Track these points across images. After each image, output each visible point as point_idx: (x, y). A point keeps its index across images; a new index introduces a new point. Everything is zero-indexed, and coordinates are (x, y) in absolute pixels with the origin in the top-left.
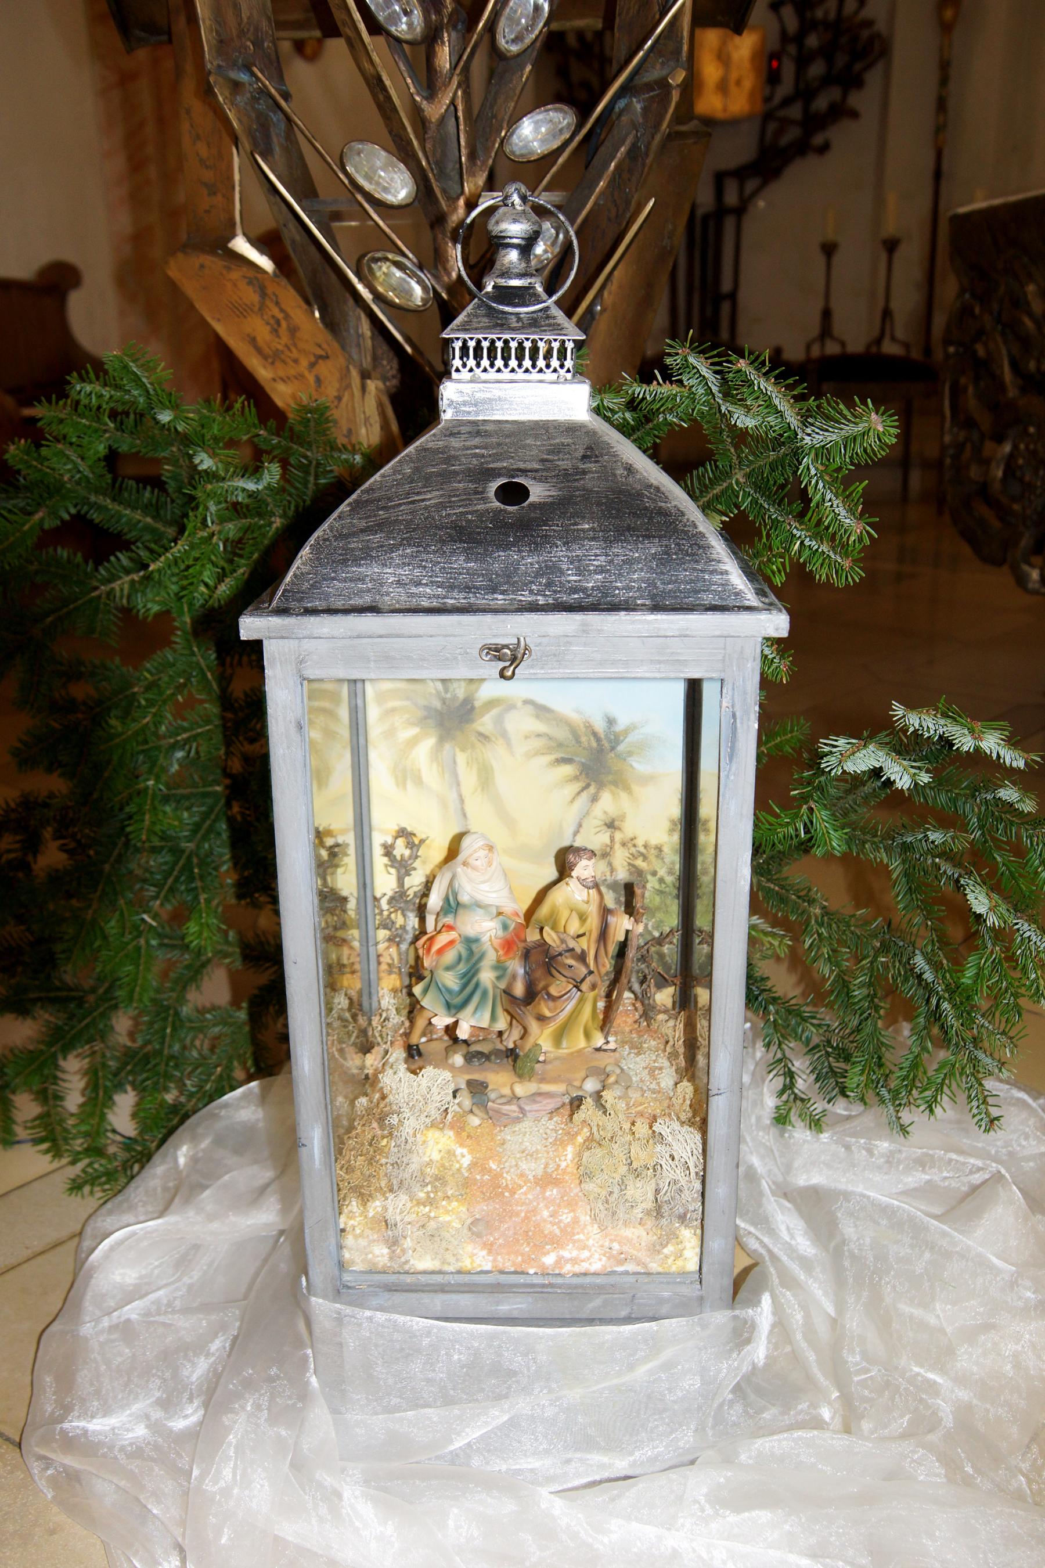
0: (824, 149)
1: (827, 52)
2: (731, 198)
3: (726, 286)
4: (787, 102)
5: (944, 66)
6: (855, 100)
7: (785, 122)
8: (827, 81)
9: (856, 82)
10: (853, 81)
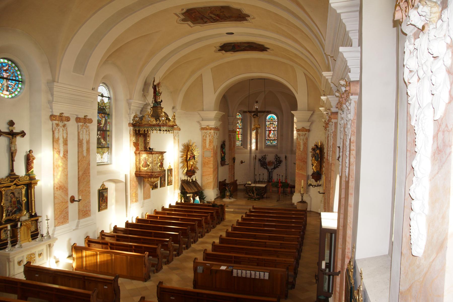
0: (278, 167)
1: (278, 161)
2: (272, 171)
3: (272, 176)
5: (286, 163)
6: (280, 164)
7: (275, 166)
8: (279, 163)
9: (281, 164)
10: (280, 163)
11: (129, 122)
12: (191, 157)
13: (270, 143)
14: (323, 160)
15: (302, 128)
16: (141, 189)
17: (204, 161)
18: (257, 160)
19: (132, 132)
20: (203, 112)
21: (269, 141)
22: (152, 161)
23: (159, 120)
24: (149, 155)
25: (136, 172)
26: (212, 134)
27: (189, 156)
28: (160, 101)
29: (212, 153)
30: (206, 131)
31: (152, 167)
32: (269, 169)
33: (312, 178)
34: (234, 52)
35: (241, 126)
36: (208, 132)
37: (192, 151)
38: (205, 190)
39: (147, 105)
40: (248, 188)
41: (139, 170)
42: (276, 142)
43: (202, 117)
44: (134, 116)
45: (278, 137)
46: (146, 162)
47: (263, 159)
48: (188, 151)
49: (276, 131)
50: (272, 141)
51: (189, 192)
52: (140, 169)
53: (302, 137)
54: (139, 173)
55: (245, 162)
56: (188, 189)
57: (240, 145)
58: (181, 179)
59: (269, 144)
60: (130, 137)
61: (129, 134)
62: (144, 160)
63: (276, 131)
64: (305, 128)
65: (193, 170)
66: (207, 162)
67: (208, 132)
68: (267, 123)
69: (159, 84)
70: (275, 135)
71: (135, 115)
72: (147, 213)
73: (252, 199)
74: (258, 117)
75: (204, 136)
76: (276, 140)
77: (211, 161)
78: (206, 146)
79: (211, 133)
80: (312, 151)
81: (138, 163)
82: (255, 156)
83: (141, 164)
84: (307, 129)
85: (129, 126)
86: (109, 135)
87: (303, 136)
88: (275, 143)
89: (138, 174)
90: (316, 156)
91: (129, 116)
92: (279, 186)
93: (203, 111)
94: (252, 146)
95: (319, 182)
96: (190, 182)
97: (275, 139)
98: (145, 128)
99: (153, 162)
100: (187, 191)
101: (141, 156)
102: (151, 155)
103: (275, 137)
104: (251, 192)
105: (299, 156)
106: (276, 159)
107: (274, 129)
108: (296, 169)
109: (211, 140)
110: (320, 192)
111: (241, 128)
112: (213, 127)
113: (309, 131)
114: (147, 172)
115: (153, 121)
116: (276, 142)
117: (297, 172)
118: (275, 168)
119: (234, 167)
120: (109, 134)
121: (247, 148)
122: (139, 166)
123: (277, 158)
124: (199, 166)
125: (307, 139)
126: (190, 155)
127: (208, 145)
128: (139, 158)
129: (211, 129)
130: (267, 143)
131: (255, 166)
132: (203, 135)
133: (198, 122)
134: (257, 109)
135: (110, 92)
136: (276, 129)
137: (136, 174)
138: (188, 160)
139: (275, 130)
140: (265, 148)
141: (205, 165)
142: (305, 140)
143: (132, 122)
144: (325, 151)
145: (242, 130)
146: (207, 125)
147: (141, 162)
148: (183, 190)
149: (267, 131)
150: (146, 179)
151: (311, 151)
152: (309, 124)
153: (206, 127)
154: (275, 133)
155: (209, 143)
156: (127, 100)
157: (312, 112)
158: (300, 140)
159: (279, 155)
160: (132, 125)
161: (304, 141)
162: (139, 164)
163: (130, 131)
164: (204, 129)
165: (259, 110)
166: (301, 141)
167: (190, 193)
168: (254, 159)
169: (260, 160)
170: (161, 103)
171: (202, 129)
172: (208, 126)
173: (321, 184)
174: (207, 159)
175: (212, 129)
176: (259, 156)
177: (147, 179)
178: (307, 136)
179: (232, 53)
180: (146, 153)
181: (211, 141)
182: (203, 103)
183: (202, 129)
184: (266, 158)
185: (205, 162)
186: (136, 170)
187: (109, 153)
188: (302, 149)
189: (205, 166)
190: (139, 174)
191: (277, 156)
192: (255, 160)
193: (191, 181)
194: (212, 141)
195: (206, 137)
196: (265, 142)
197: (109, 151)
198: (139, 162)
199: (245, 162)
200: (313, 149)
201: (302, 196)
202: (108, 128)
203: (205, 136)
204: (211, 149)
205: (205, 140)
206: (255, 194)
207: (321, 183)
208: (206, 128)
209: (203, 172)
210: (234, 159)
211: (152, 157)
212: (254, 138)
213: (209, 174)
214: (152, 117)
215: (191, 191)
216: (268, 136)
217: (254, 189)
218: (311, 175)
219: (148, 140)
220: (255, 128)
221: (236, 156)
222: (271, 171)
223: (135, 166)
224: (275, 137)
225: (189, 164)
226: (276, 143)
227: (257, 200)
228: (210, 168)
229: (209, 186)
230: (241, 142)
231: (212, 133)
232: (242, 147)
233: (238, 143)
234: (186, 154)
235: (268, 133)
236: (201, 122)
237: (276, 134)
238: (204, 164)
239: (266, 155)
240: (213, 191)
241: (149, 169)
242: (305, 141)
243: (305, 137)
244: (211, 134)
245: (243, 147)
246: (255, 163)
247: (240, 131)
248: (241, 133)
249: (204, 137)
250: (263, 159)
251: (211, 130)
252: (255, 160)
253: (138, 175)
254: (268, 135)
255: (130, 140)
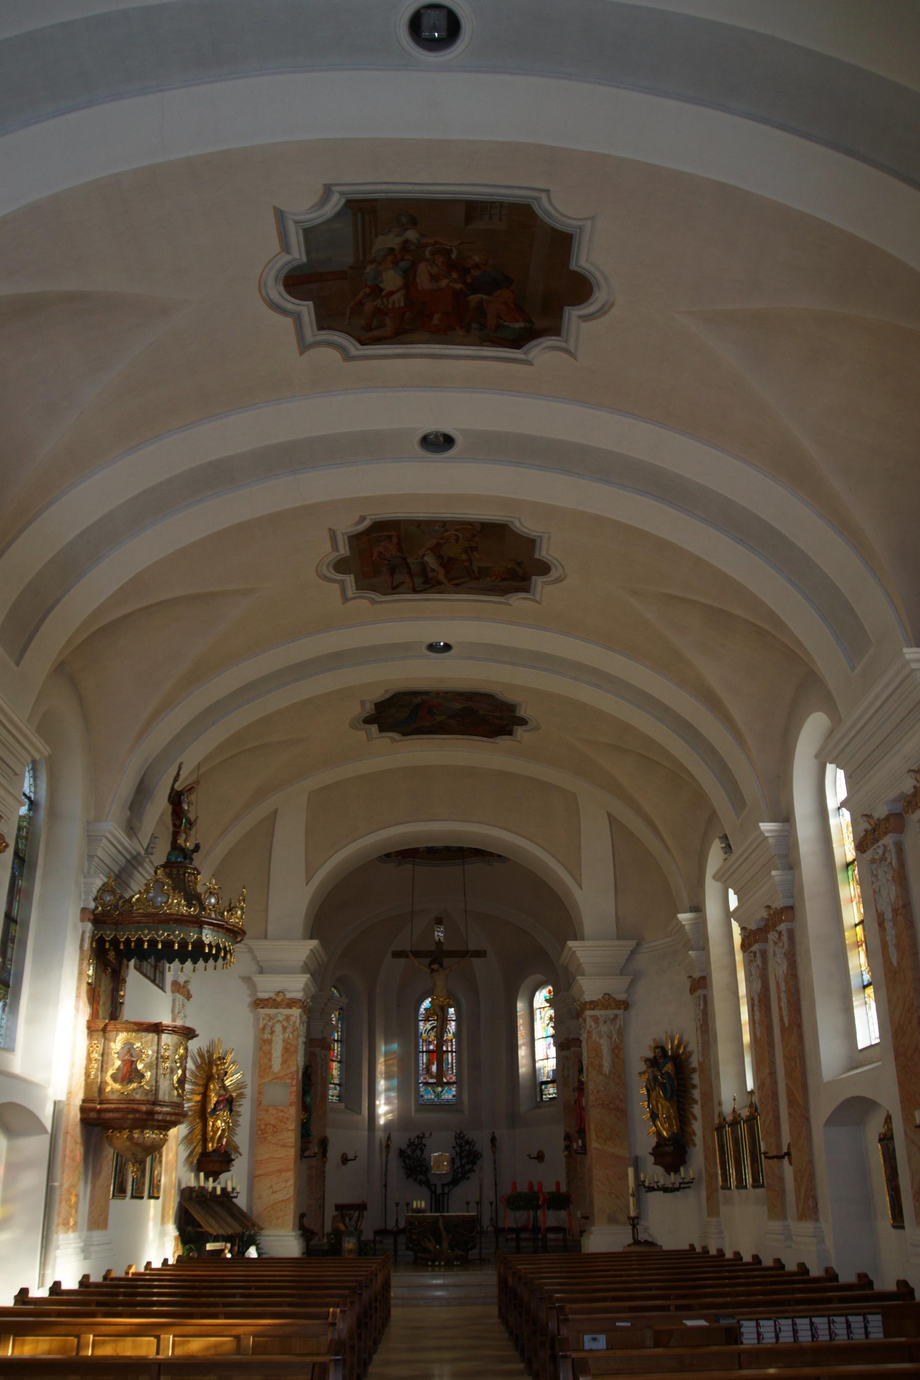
0: (468, 1178)
2: (446, 1191)
4: (458, 1168)
5: (494, 1160)
9: (476, 1164)
10: (473, 1163)
11: (82, 906)
12: (222, 1101)
13: (433, 1097)
14: (692, 1094)
15: (603, 998)
16: (86, 1182)
17: (261, 1120)
18: (393, 1154)
19: (87, 946)
20: (265, 942)
21: (430, 1089)
22: (154, 1058)
23: (197, 905)
24: (144, 1034)
25: (84, 1101)
26: (295, 1022)
27: (214, 1099)
28: (192, 848)
29: (294, 1089)
30: (273, 1011)
31: (154, 1084)
32: (435, 1185)
33: (656, 1163)
34: (405, 734)
35: (339, 1033)
36: (279, 1015)
37: (223, 1080)
38: (265, 1232)
39: (134, 862)
40: (416, 1223)
41: (96, 1095)
42: (454, 1089)
43: (258, 963)
44: (103, 885)
45: (459, 1074)
46: (132, 1063)
47: (414, 1151)
48: (209, 1078)
49: (452, 1052)
50: (440, 1089)
51: (215, 1234)
52: (101, 1090)
53: (604, 1028)
54: (98, 1107)
55: (356, 1157)
56: (210, 1226)
57: (335, 1098)
58: (180, 1184)
59: (429, 1097)
60: (81, 960)
61: (78, 951)
62: (122, 1056)
63: (452, 1052)
64: (615, 996)
65: (226, 1152)
66: (273, 1122)
67: (281, 1014)
68: (421, 1027)
69: (190, 789)
70: (450, 1066)
71: (105, 880)
72: (130, 1267)
73: (437, 1263)
74: (447, 971)
75: (264, 1029)
76: (454, 1083)
77: (288, 1119)
78: (271, 1067)
79: (290, 1020)
80: (648, 1067)
81: (96, 1066)
82: (388, 1140)
83: (106, 1072)
84: (619, 1001)
85: (82, 920)
86: (15, 936)
87: (608, 1022)
88: (449, 1094)
89: (94, 1109)
90: (662, 1083)
91: (85, 884)
92: (540, 1203)
93: (266, 938)
94: (377, 1102)
95: (686, 1170)
96: (217, 1196)
97: (452, 1081)
98: (142, 930)
99: (157, 1064)
100: (208, 1229)
101: (109, 1040)
102: (154, 1034)
103: (450, 1072)
104: (431, 1238)
105: (598, 1092)
106: (458, 1149)
107: (447, 1048)
108: (593, 1137)
109: (288, 1043)
110: (769, 1155)
111: (337, 1041)
112: (300, 995)
113: (625, 1005)
114: (133, 1101)
115: (179, 904)
116: (454, 1090)
117: (596, 1149)
118: (455, 1182)
119: (324, 1172)
120: (14, 933)
121: (359, 1112)
122: (99, 1080)
123: (464, 1144)
124: (242, 1139)
125: (621, 1033)
126: (216, 1094)
127: (280, 1061)
128: (104, 1049)
129: (291, 1004)
130: (422, 1093)
131: (386, 1176)
132: (261, 1026)
133: (247, 980)
134: (439, 943)
135: (38, 782)
136: (452, 1045)
137: (83, 1110)
138: (209, 1110)
139: (449, 1049)
140: (416, 1111)
141: (265, 1135)
142: (615, 1036)
143: (92, 905)
144: (694, 1062)
145: (341, 1047)
146: (278, 989)
147: (107, 1064)
148: (190, 1229)
149: (423, 1052)
150: (119, 1132)
151: (642, 1067)
152: (624, 982)
153: (272, 995)
154: (450, 1061)
155: (283, 1055)
156: (88, 822)
157: (633, 943)
158: (600, 1039)
159: (470, 1135)
160: (92, 917)
161: (613, 1039)
162: (102, 1071)
163: (82, 940)
164: (266, 1005)
165: (446, 947)
166: (603, 1041)
167: (216, 1239)
168: (384, 1149)
169: (402, 1153)
170: (195, 856)
171: (259, 1003)
172: (281, 994)
173: (693, 1179)
174: (274, 1112)
175: (294, 1002)
176: (400, 1141)
177: (126, 1134)
178: (622, 1023)
179: (396, 741)
180: (136, 1028)
181: (289, 1046)
182: (266, 910)
183: (259, 1003)
184: (425, 1146)
185: (266, 1125)
186: (85, 1094)
187: (7, 1008)
188: (607, 1068)
189: (265, 1138)
190: (99, 1111)
191: (461, 1138)
192: (388, 1153)
193: (219, 1192)
194: (293, 1049)
195: (272, 1033)
196: (417, 1090)
197: (7, 1001)
198: (102, 1061)
199: (356, 1157)
200: (653, 1063)
201: (634, 1226)
202: (15, 909)
203: (268, 1031)
204: (290, 1076)
205: (269, 1042)
206: (445, 1244)
207: (691, 1174)
208: (275, 1000)
209: (254, 1164)
210: (324, 1143)
211: (158, 1044)
212: (383, 1076)
213: (280, 1171)
214: (174, 889)
215: (221, 1232)
216: (424, 1072)
217: (441, 1226)
218: (651, 1151)
219: (122, 993)
220: (438, 1010)
221: (330, 1133)
222: (443, 1194)
223: (83, 1078)
224: (450, 1072)
225: (210, 1129)
226: (454, 1093)
227: (455, 1263)
228: (283, 1146)
229: (278, 1218)
230: (338, 1088)
231: (293, 1019)
232: (342, 1105)
233: (333, 1093)
234: (201, 1089)
235: (425, 1061)
236: (258, 979)
237: (454, 1065)
238: (259, 1134)
239: (424, 1135)
240: (294, 1234)
241: (141, 1090)
242: (617, 1040)
243: (614, 1026)
244: (291, 1022)
245: (346, 1108)
246: (387, 1163)
247: (336, 1051)
248: (339, 1057)
249: (266, 1032)
250: (414, 1151)
251: (291, 1008)
252: (388, 1153)
253: (93, 1115)
254: (424, 1066)
255: (80, 973)
